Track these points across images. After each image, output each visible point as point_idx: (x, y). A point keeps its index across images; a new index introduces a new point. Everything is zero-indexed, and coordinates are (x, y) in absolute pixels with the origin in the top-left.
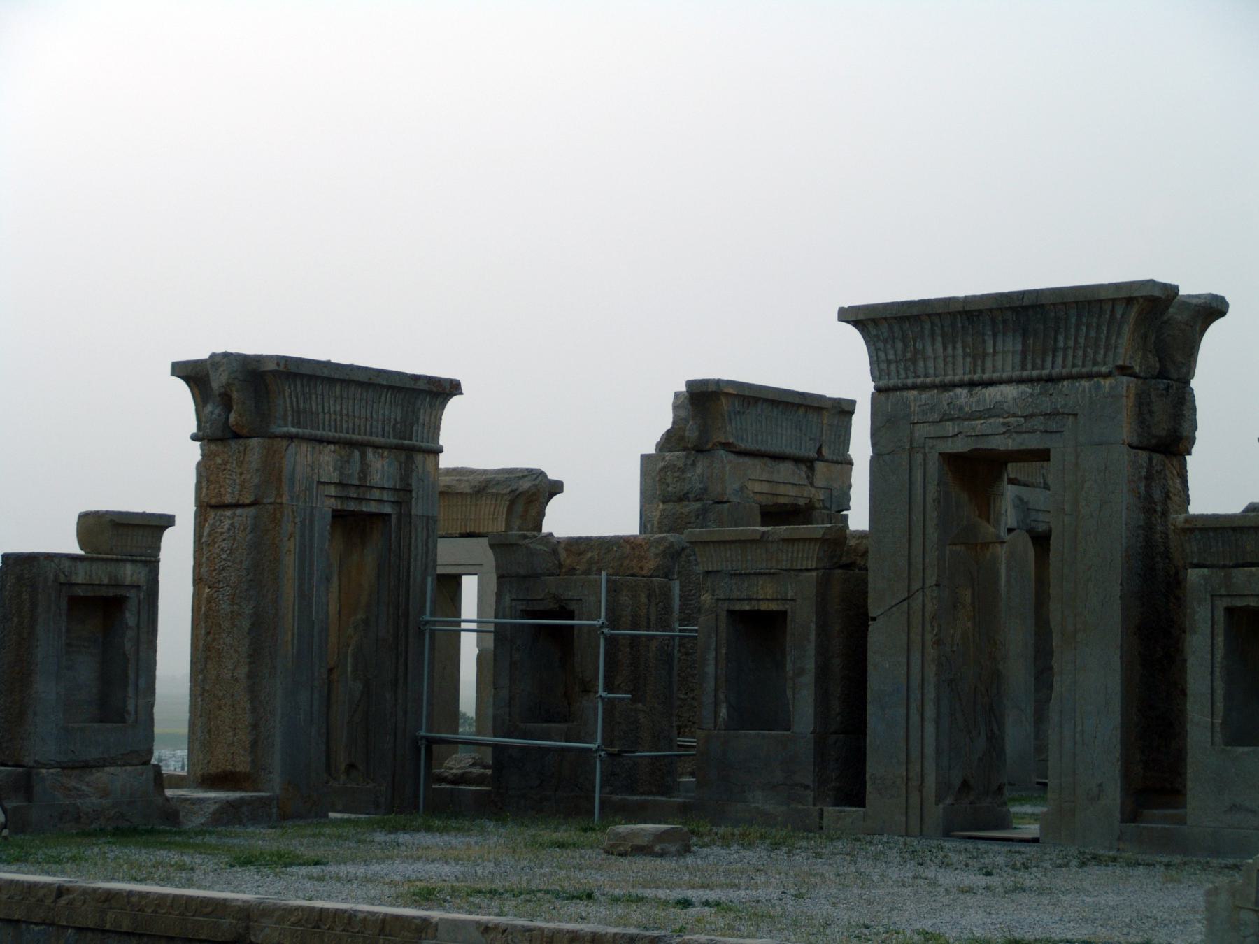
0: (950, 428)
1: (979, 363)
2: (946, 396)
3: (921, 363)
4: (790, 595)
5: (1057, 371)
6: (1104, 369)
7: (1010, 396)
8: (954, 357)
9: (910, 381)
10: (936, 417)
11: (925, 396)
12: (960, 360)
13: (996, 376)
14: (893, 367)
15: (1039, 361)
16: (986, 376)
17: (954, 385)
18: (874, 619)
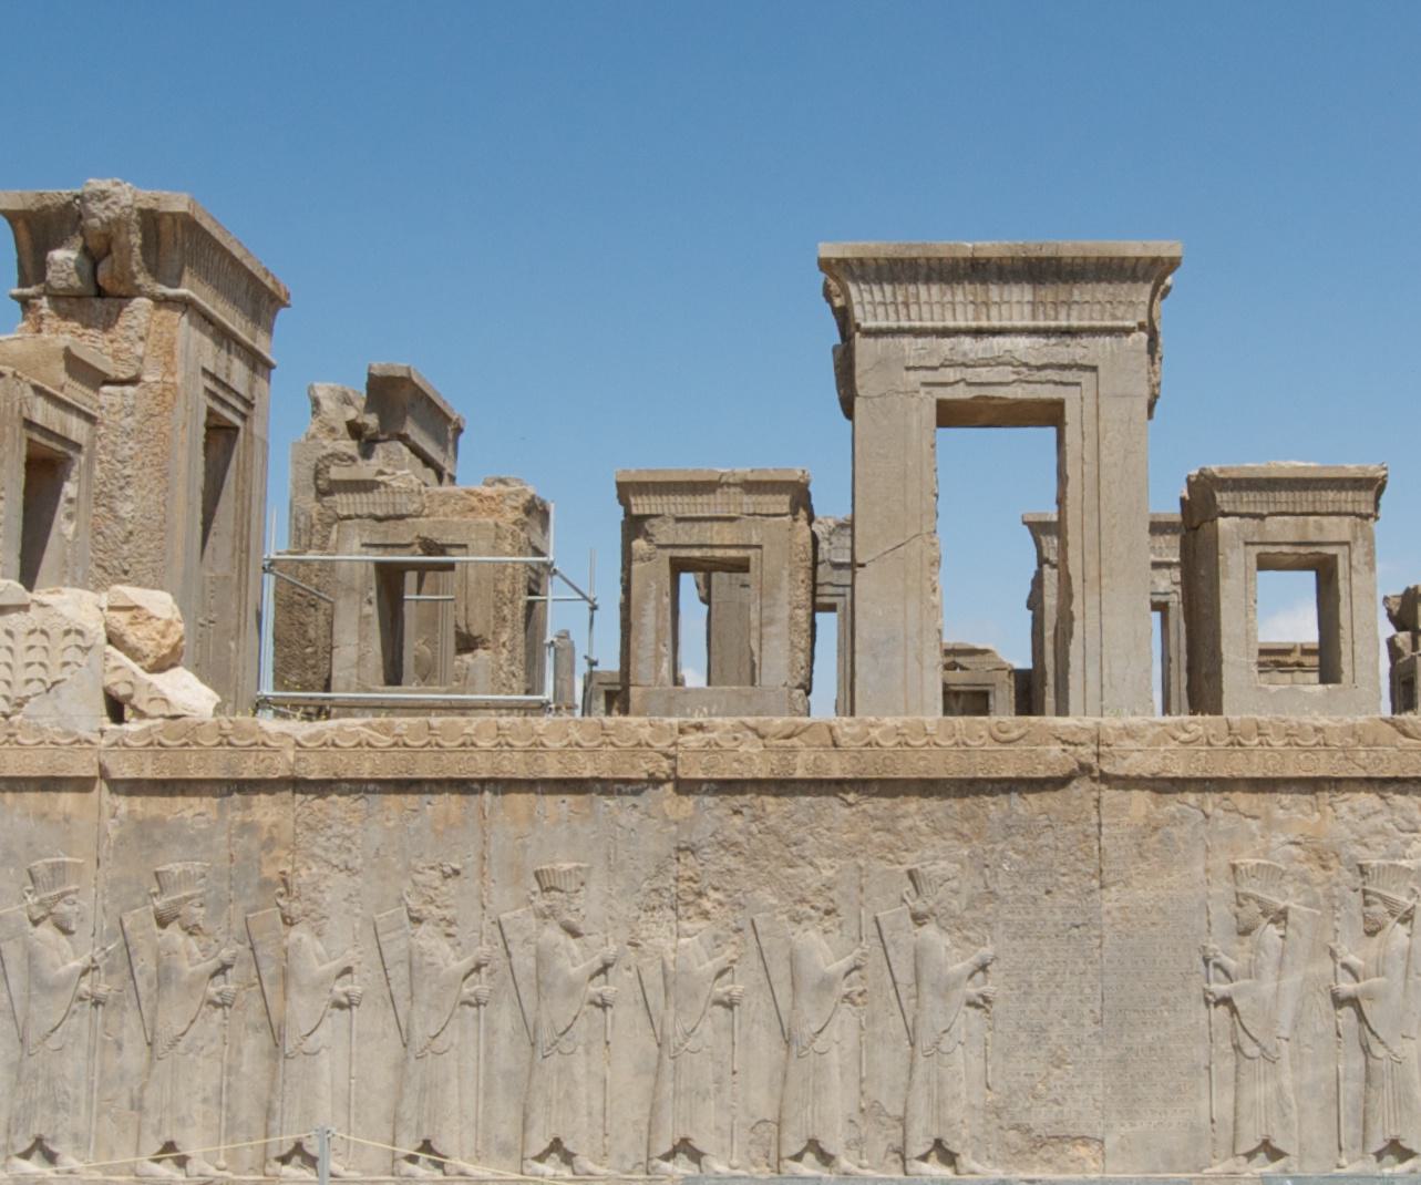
0: (951, 374)
1: (984, 310)
2: (947, 342)
3: (914, 309)
4: (755, 541)
5: (1075, 323)
6: (1129, 323)
7: (1021, 346)
8: (953, 303)
9: (905, 324)
10: (935, 362)
11: (921, 341)
12: (959, 309)
13: (1006, 324)
14: (881, 310)
15: (1052, 313)
16: (996, 323)
17: (956, 332)
18: (863, 566)
